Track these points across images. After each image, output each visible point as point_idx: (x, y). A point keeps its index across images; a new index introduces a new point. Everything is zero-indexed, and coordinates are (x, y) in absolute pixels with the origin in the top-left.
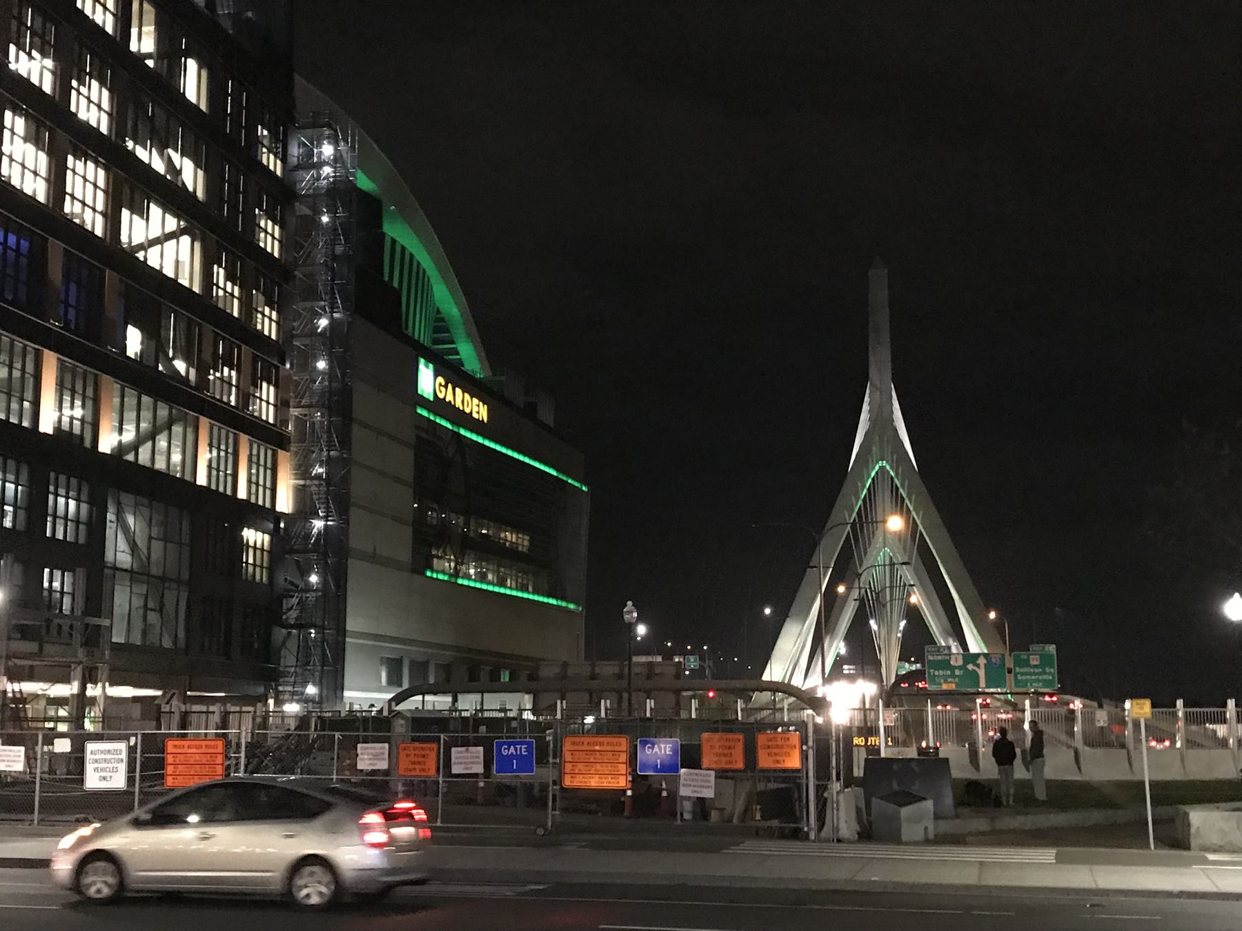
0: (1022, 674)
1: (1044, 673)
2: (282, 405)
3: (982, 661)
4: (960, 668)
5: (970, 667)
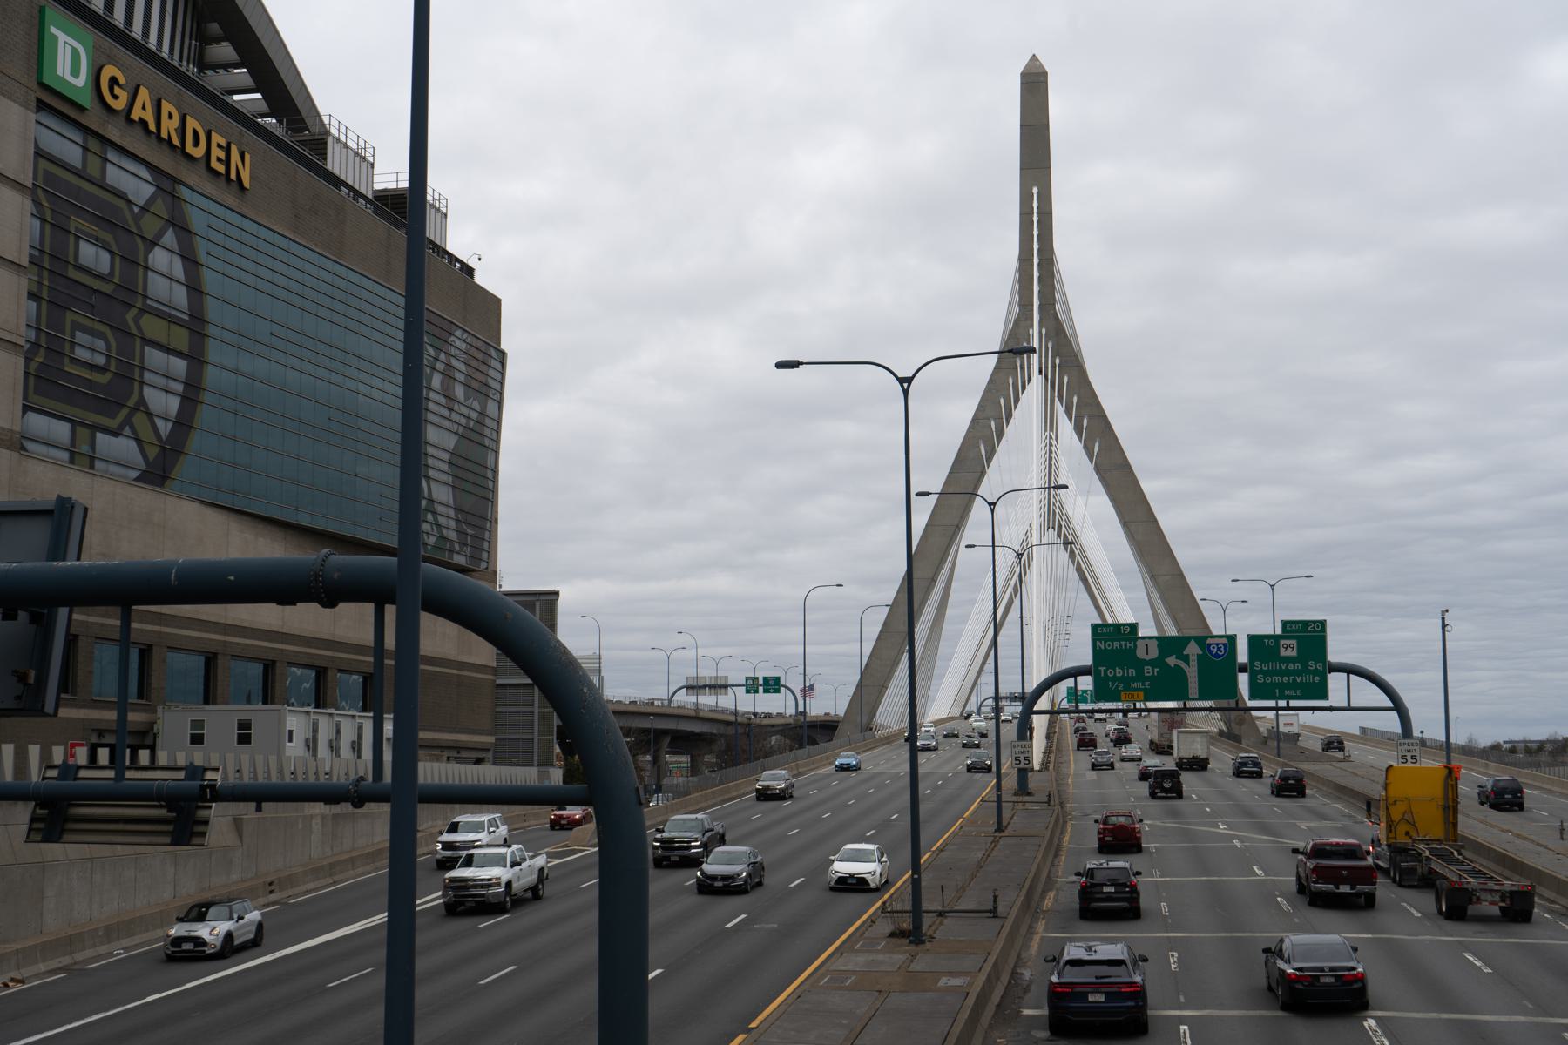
0: (1266, 673)
1: (1305, 670)
2: (39, 49)
3: (1193, 650)
4: (1151, 663)
5: (1172, 661)
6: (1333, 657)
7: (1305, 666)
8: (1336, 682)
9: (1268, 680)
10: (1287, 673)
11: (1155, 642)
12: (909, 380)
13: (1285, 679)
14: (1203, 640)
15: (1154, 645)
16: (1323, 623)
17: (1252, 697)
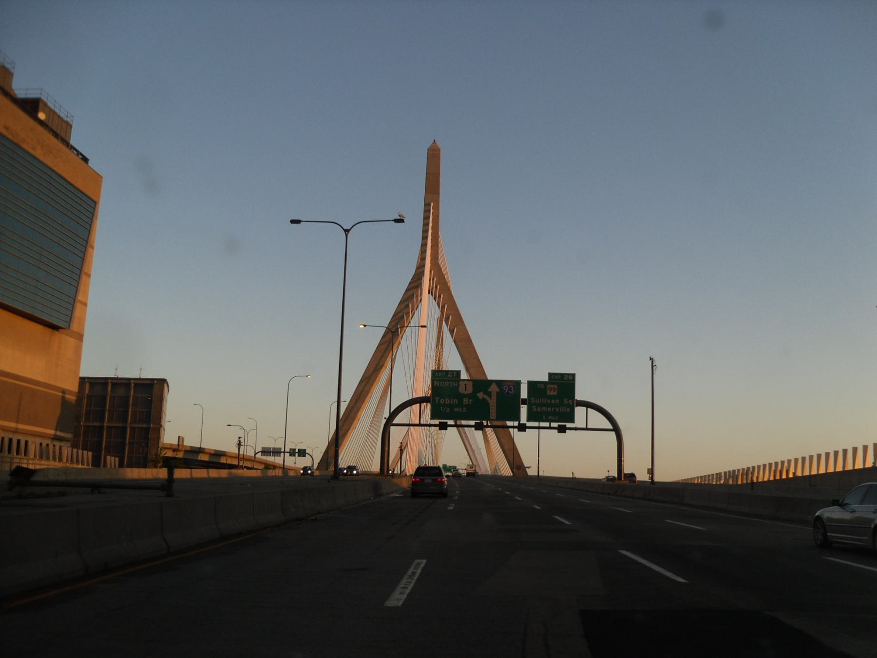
0: (538, 405)
3: (494, 389)
4: (468, 396)
5: (480, 395)
6: (579, 396)
8: (580, 411)
9: (539, 409)
11: (471, 383)
15: (470, 385)
16: (574, 375)
17: (529, 420)
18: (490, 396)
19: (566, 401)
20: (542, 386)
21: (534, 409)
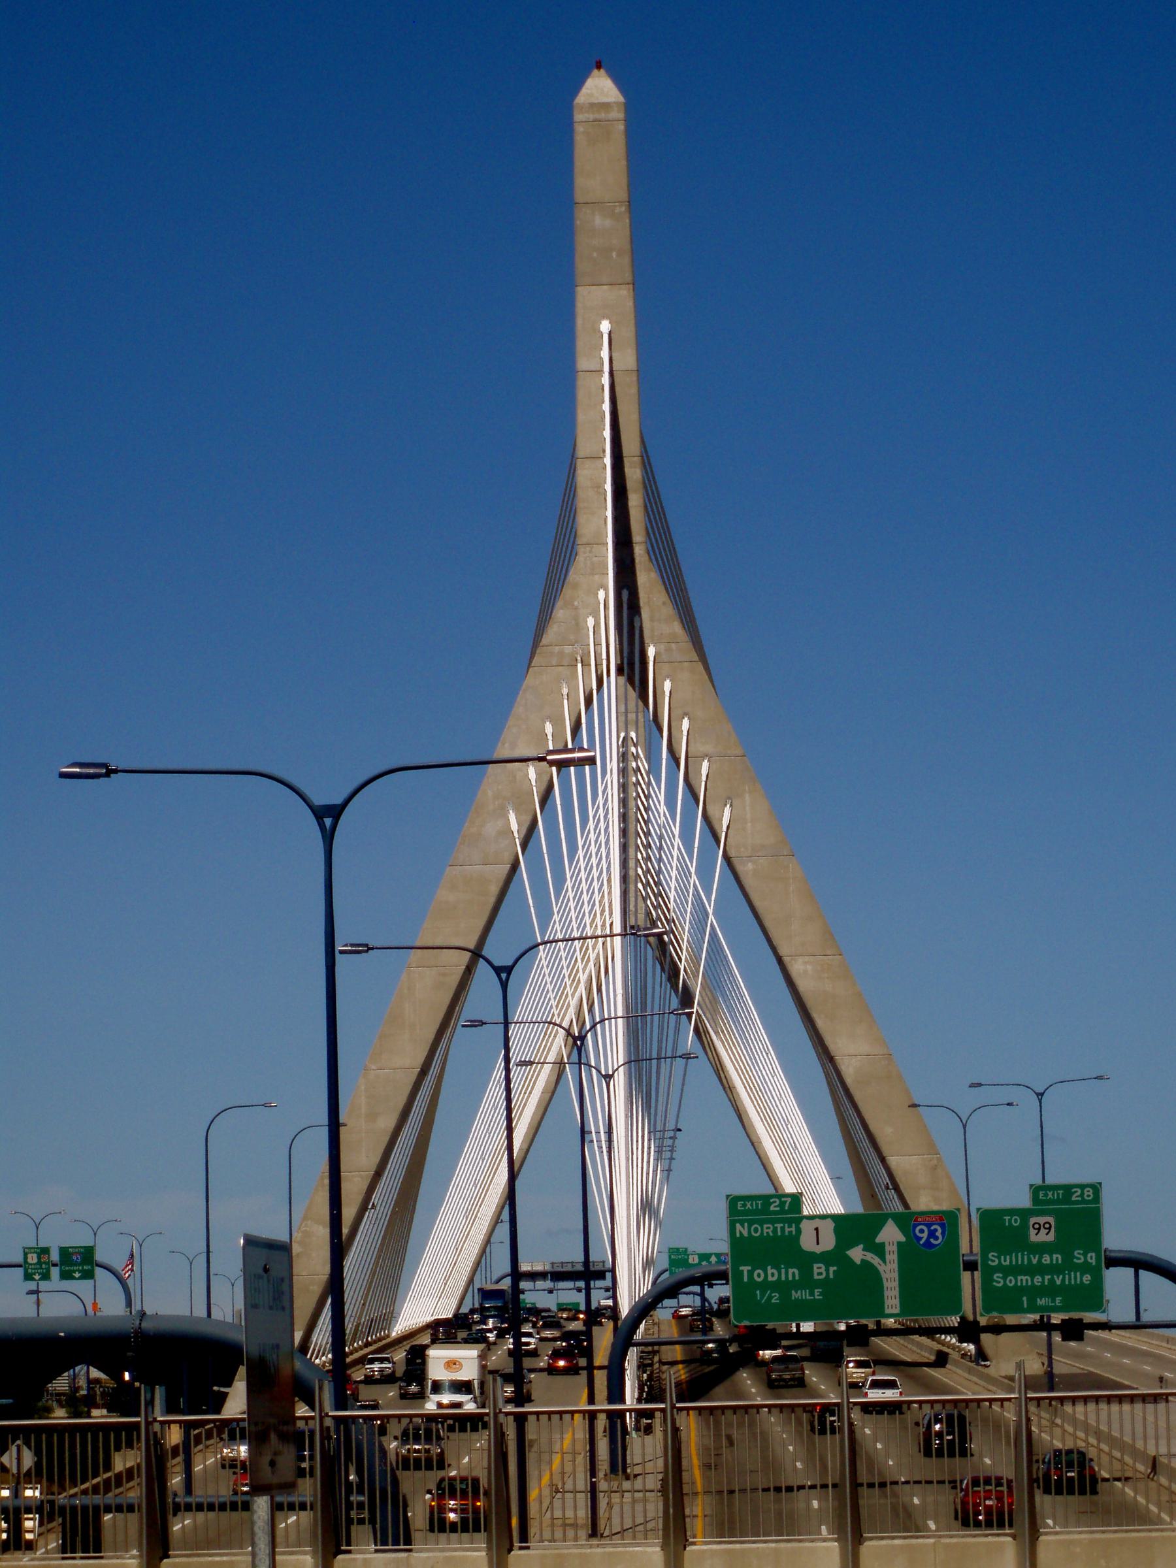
0: (1007, 1271)
1: (1068, 1265)
5: (857, 1254)
7: (1068, 1257)
8: (1118, 1281)
10: (1041, 1270)
12: (335, 812)
13: (1038, 1280)
14: (907, 1220)
15: (828, 1228)
16: (1096, 1188)
18: (882, 1257)
19: (1079, 1257)
20: (1016, 1222)
21: (998, 1280)
